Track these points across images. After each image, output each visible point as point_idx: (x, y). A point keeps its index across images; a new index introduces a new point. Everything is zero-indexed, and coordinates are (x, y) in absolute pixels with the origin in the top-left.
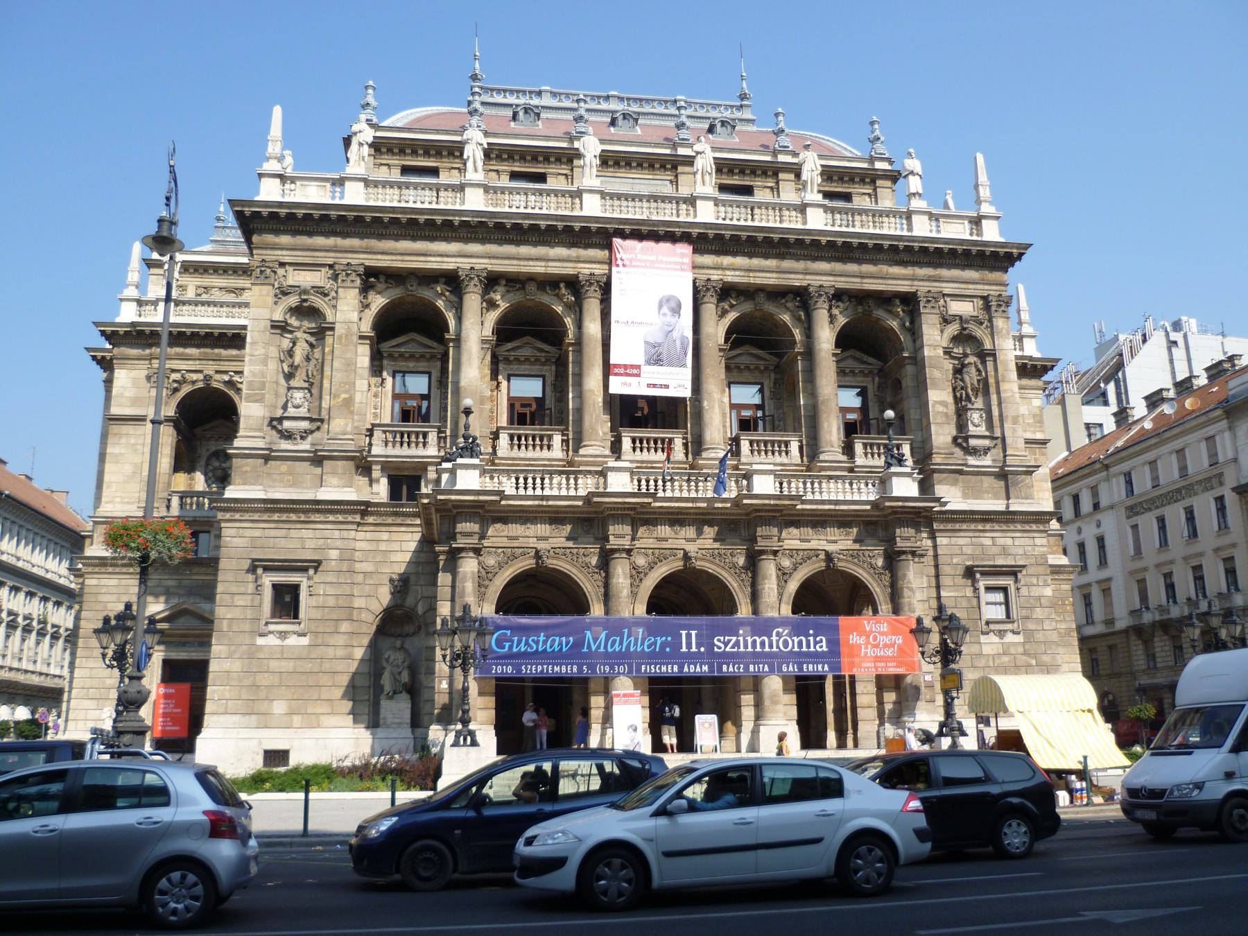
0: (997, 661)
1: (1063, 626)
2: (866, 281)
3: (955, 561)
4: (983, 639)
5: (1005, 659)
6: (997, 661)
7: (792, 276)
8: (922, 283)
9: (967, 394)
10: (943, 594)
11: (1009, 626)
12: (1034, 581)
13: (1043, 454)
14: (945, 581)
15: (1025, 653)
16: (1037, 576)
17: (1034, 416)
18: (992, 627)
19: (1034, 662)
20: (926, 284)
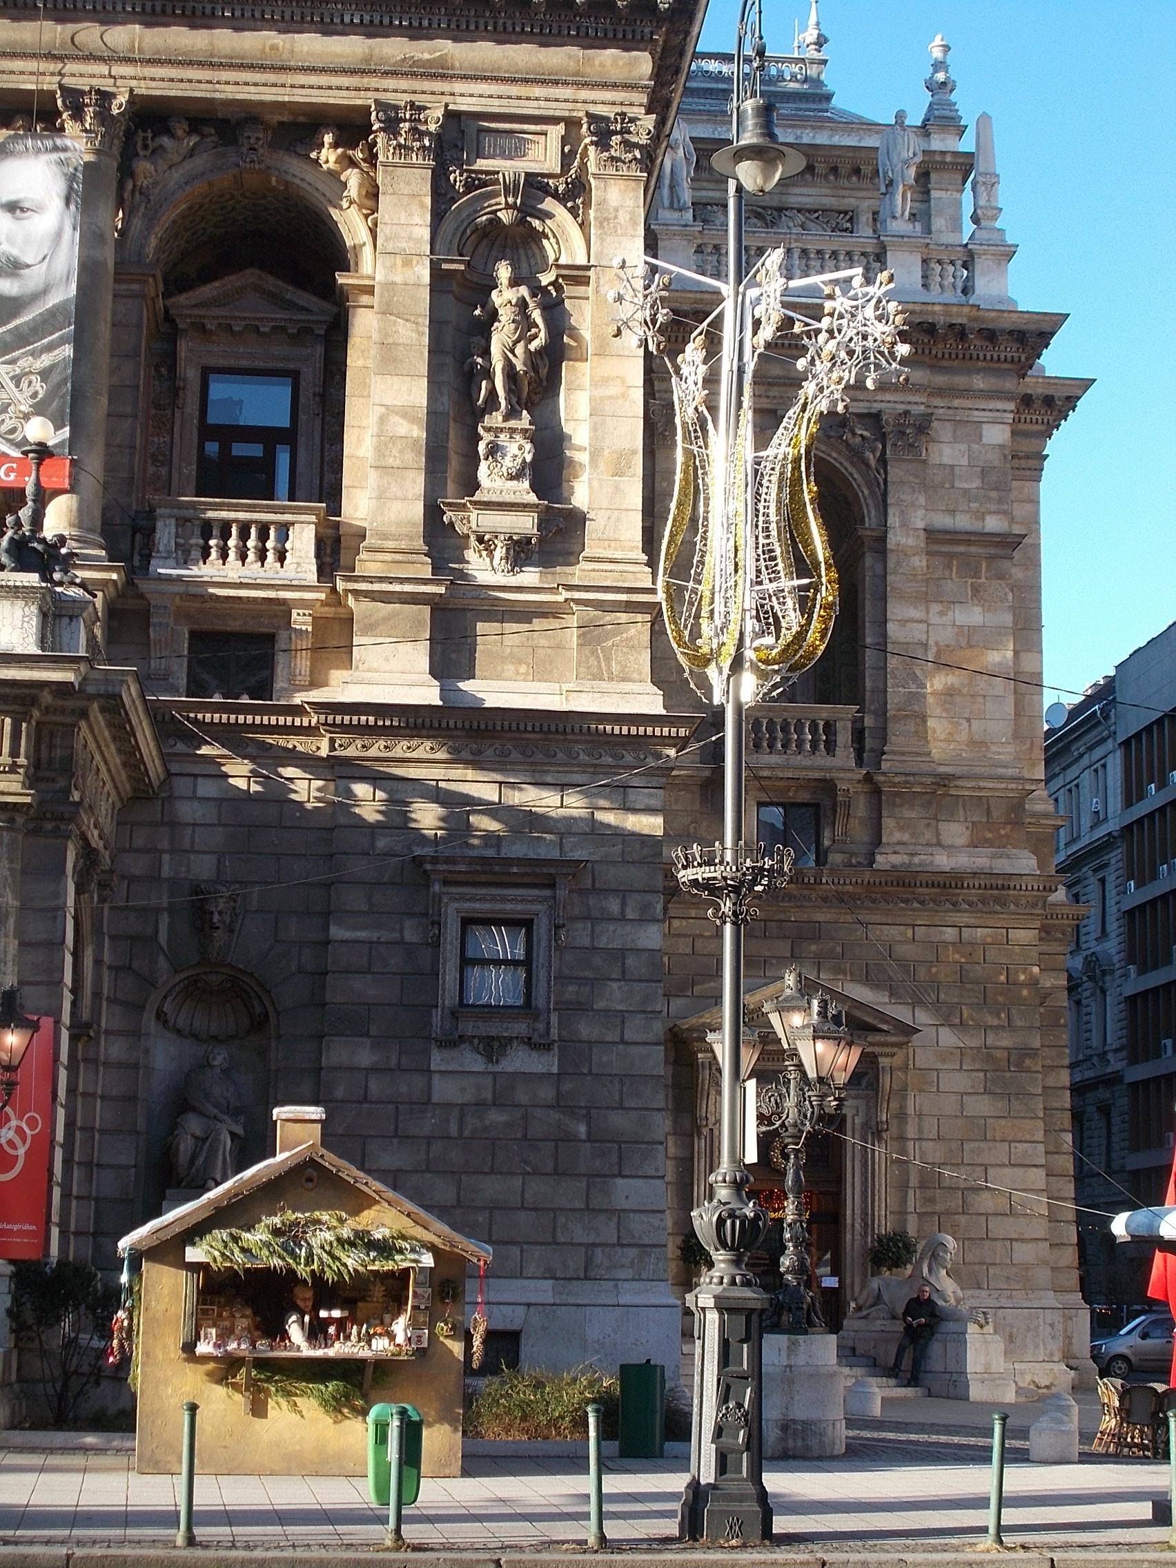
0: (471, 1122)
1: (1006, 1041)
2: (226, 75)
3: (381, 844)
4: (437, 1059)
5: (497, 1117)
6: (471, 1122)
7: (18, 65)
8: (390, 83)
9: (492, 392)
10: (337, 932)
11: (520, 1028)
12: (614, 906)
13: (1001, 576)
14: (355, 899)
15: (557, 1104)
16: (623, 894)
17: (984, 472)
18: (468, 1027)
19: (582, 1129)
20: (404, 84)
